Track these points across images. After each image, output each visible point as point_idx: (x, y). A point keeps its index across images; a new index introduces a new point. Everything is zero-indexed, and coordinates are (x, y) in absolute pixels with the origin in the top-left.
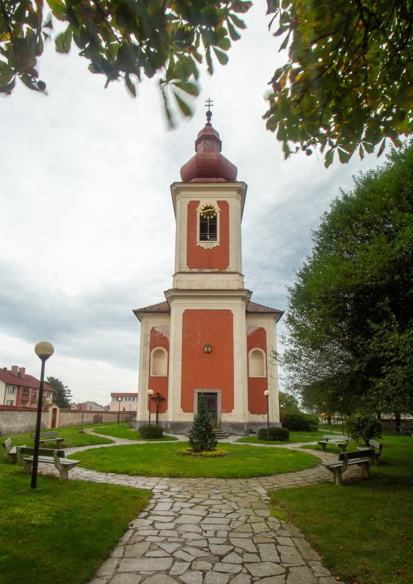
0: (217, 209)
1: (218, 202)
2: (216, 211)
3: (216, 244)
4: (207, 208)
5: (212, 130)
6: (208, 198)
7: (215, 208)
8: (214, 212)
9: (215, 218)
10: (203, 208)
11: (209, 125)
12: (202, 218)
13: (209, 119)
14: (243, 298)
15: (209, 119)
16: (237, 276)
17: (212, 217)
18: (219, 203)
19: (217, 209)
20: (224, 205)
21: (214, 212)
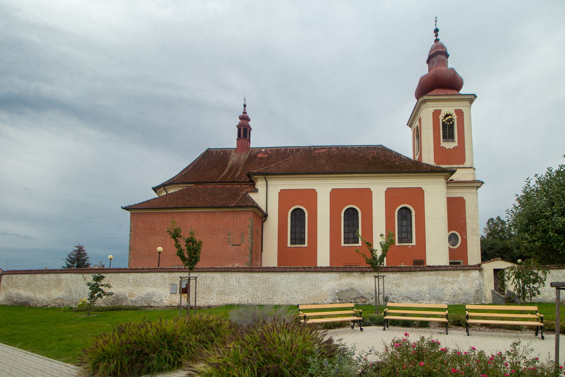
0: (455, 117)
1: (456, 111)
2: (454, 118)
4: (447, 115)
6: (448, 108)
7: (453, 115)
8: (452, 119)
9: (453, 123)
10: (444, 116)
11: (437, 40)
12: (443, 123)
13: (436, 36)
15: (436, 36)
16: (472, 170)
17: (451, 123)
18: (456, 111)
19: (455, 117)
20: (460, 113)
21: (452, 119)
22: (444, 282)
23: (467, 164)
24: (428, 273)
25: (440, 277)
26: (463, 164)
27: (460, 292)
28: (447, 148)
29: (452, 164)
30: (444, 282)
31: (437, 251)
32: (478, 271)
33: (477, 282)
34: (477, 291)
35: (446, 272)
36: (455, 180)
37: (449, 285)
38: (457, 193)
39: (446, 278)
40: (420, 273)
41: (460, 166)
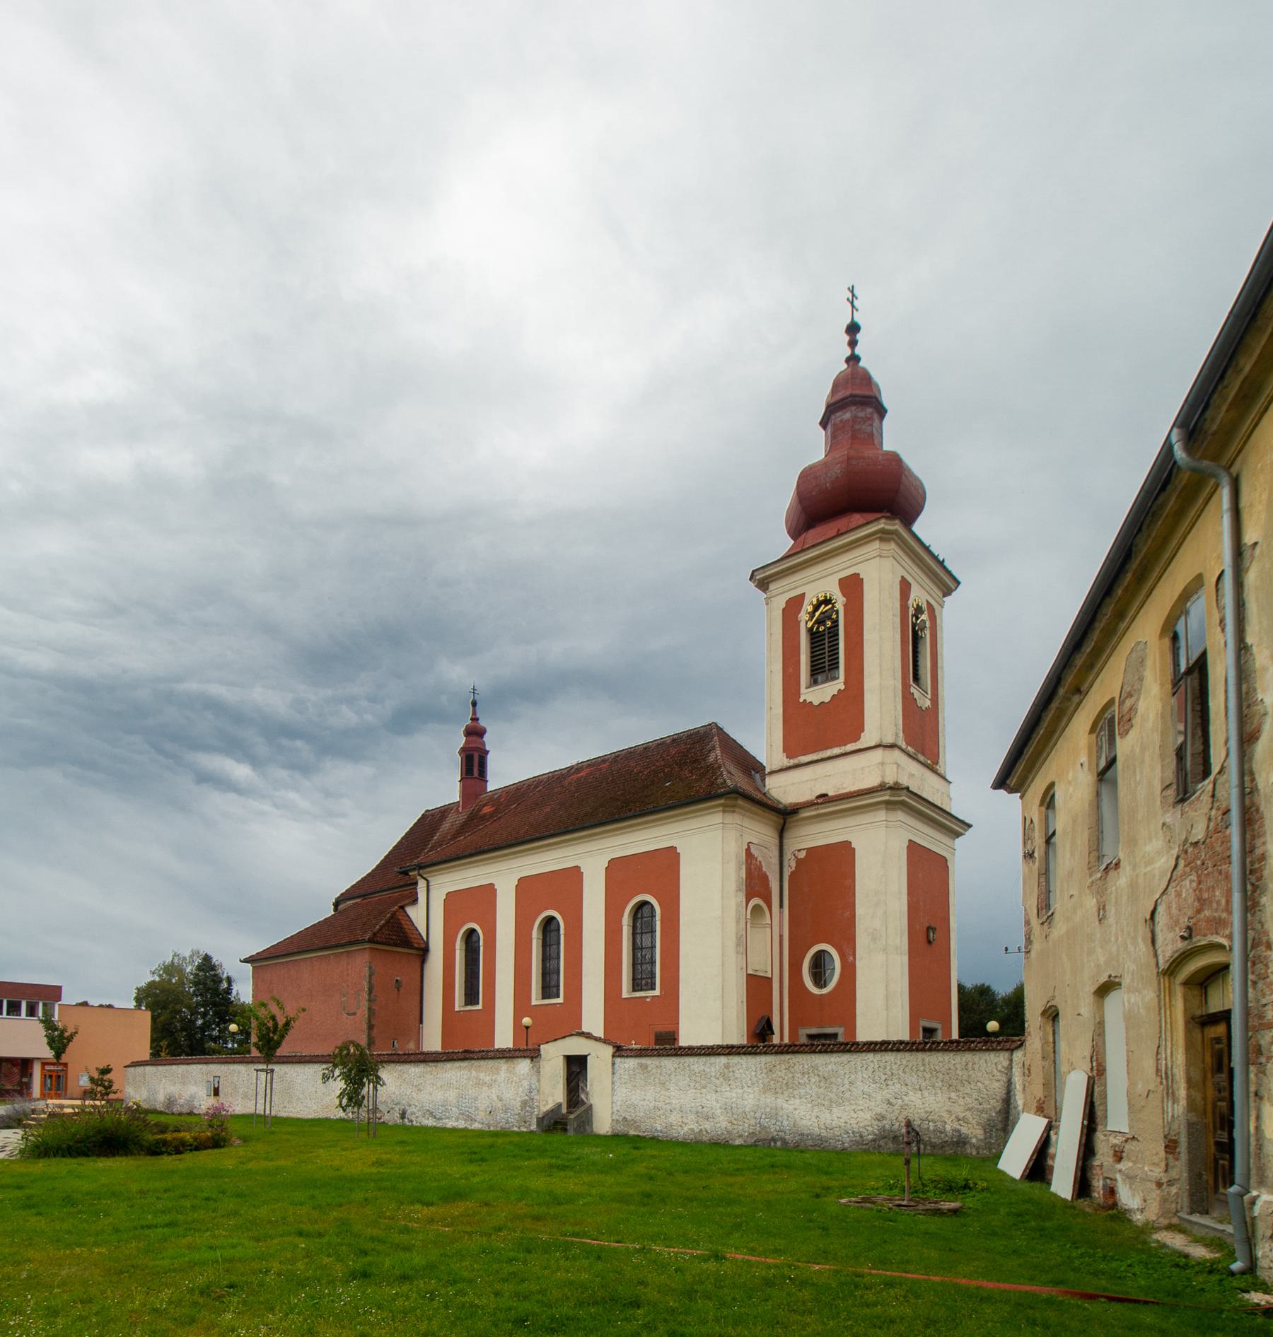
3: (837, 686)
5: (866, 379)
14: (889, 805)
22: (479, 1083)
23: (868, 738)
24: (457, 1064)
25: (474, 1073)
26: (857, 738)
27: (499, 1105)
28: (816, 703)
29: (827, 748)
30: (479, 1083)
31: (882, 1004)
32: (528, 1061)
33: (525, 1083)
34: (524, 1104)
35: (482, 1063)
36: (831, 794)
37: (485, 1088)
38: (812, 836)
39: (482, 1075)
40: (449, 1065)
41: (850, 747)
